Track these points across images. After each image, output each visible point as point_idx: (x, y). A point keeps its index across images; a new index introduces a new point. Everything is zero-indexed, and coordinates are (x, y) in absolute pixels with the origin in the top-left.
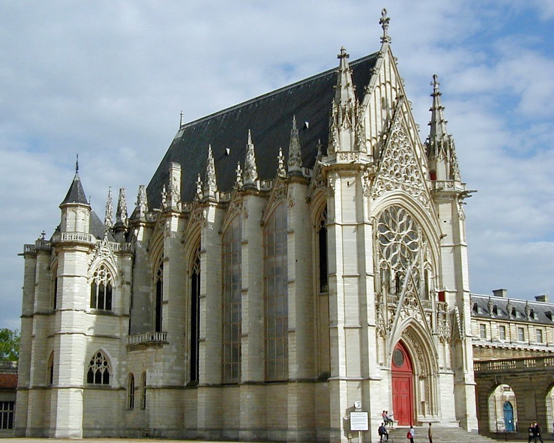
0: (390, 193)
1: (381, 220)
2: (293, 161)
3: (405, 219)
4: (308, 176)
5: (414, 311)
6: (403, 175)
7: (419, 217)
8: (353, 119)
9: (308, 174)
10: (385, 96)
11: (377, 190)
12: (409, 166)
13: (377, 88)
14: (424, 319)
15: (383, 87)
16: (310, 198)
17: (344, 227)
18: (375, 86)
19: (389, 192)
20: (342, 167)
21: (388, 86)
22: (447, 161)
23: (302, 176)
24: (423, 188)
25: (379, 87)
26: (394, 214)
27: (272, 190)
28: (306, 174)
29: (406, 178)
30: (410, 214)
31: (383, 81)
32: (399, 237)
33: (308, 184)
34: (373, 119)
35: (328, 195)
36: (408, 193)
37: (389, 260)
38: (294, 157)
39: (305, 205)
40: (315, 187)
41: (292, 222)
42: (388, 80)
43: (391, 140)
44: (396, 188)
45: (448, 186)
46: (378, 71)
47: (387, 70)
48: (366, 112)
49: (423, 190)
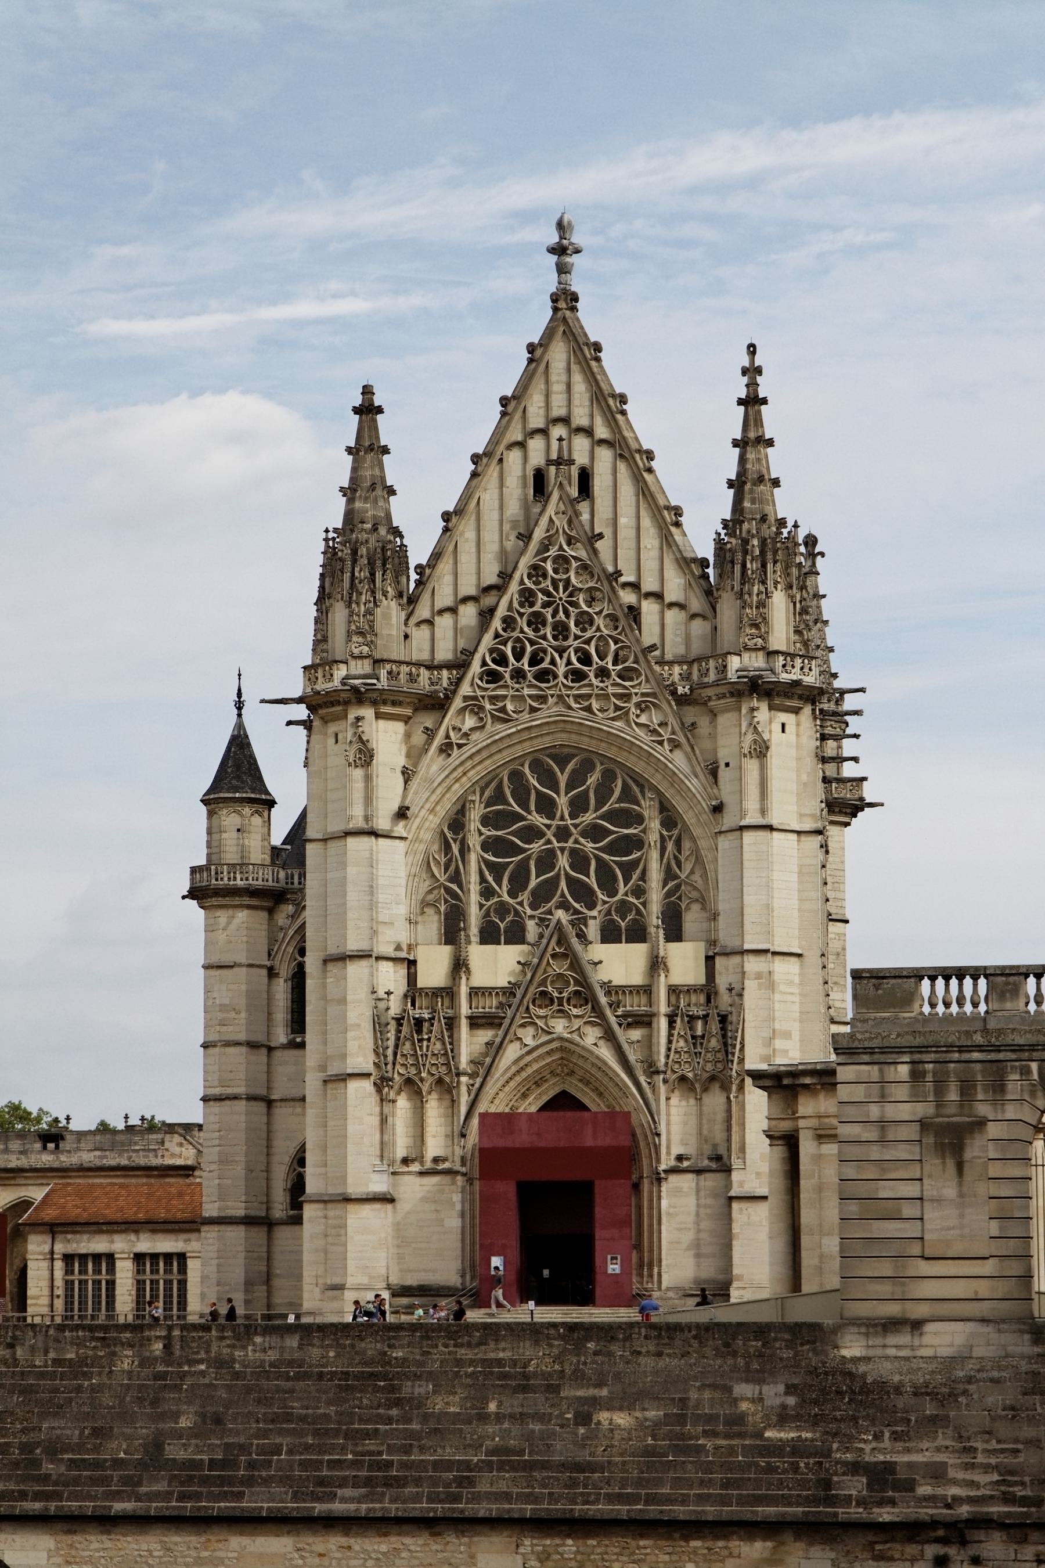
1: (498, 797)
3: (592, 780)
5: (570, 1020)
6: (561, 669)
7: (639, 767)
14: (609, 1036)
24: (645, 689)
25: (522, 445)
29: (578, 676)
31: (536, 421)
32: (563, 834)
37: (525, 897)
42: (562, 412)
44: (533, 710)
47: (558, 387)
49: (643, 695)
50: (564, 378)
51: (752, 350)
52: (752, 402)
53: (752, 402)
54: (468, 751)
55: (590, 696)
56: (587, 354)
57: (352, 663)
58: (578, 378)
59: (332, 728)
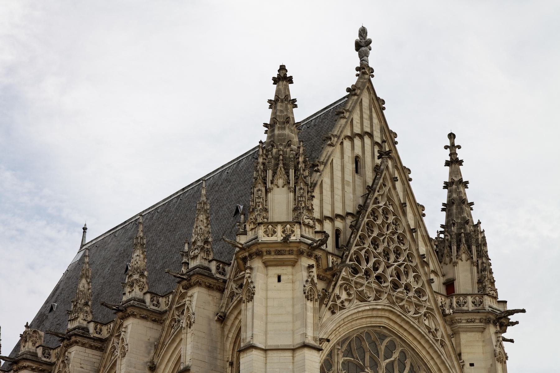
0: (364, 306)
2: (196, 251)
3: (396, 355)
4: (222, 277)
6: (390, 279)
8: (292, 172)
9: (223, 273)
10: (360, 154)
11: (339, 297)
12: (403, 267)
13: (347, 139)
15: (357, 141)
16: (225, 314)
17: (270, 354)
18: (342, 137)
19: (363, 304)
20: (268, 249)
21: (367, 140)
22: (472, 263)
23: (211, 276)
26: (374, 344)
27: (170, 308)
28: (220, 273)
30: (407, 348)
31: (357, 130)
33: (221, 291)
34: (338, 185)
35: (244, 299)
36: (399, 309)
38: (199, 243)
39: (216, 326)
40: (232, 295)
41: (189, 352)
42: (368, 130)
43: (366, 220)
45: (473, 303)
46: (348, 113)
47: (366, 116)
48: (324, 173)
49: (428, 309)
50: (368, 112)
51: (452, 136)
52: (454, 162)
53: (454, 162)
54: (345, 313)
55: (402, 300)
56: (379, 105)
57: (303, 227)
58: (374, 115)
59: (274, 271)
